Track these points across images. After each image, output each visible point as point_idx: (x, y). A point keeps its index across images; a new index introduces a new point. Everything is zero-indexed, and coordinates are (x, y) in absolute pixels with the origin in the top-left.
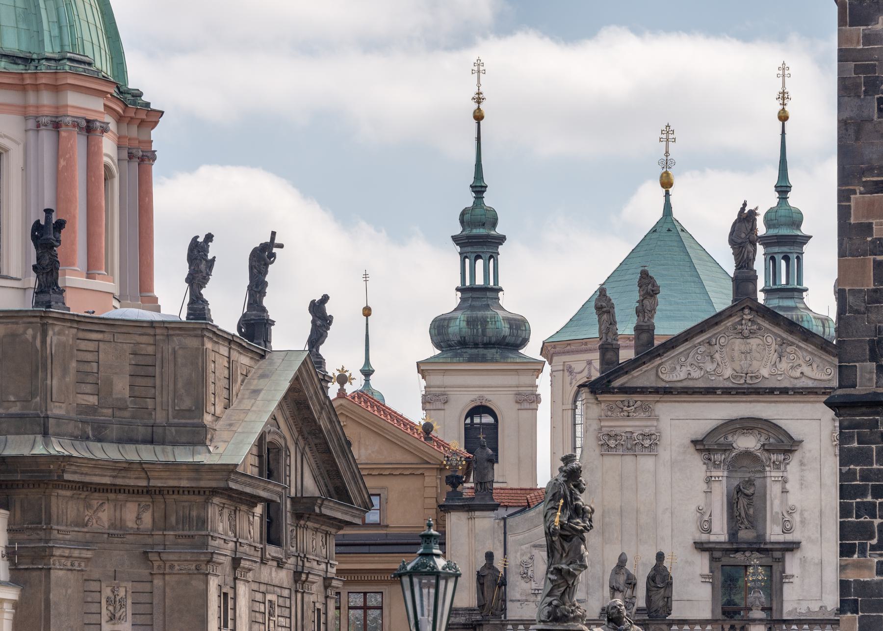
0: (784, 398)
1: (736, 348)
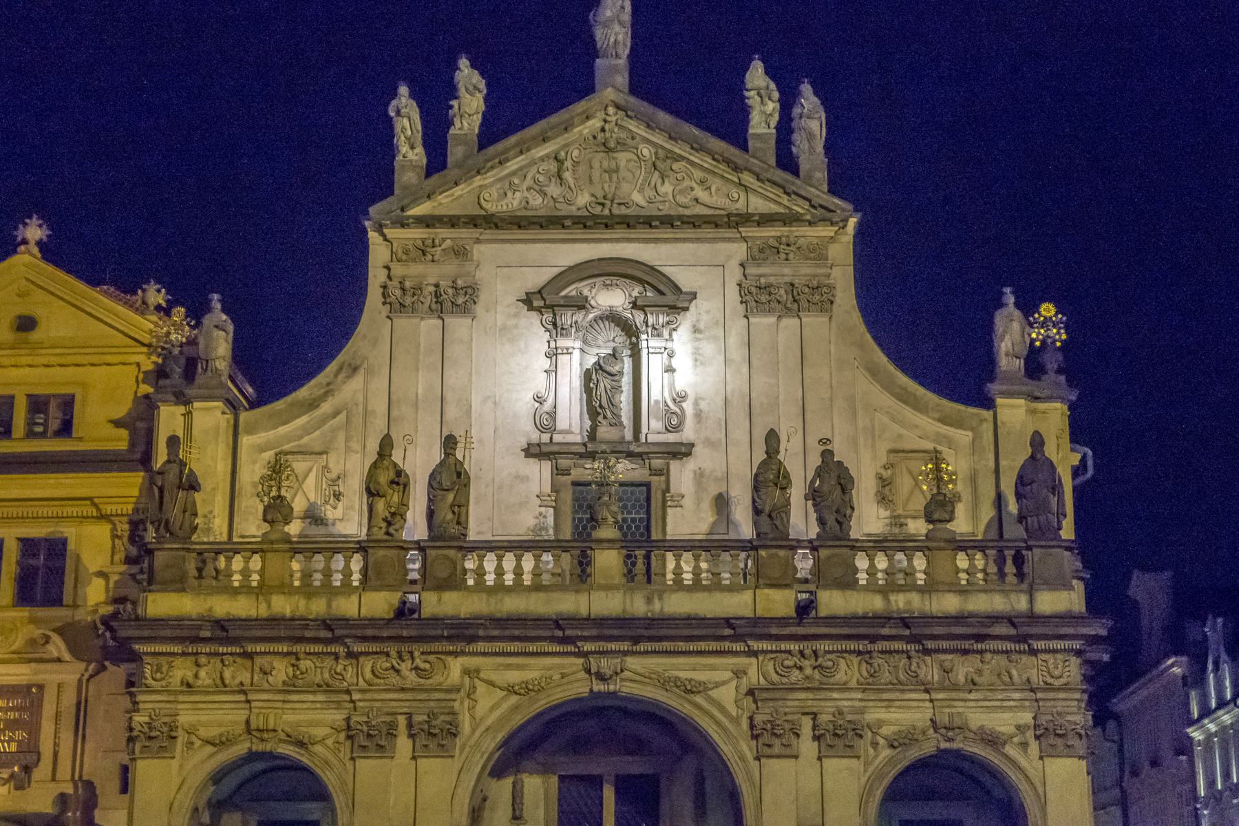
1: (596, 165)
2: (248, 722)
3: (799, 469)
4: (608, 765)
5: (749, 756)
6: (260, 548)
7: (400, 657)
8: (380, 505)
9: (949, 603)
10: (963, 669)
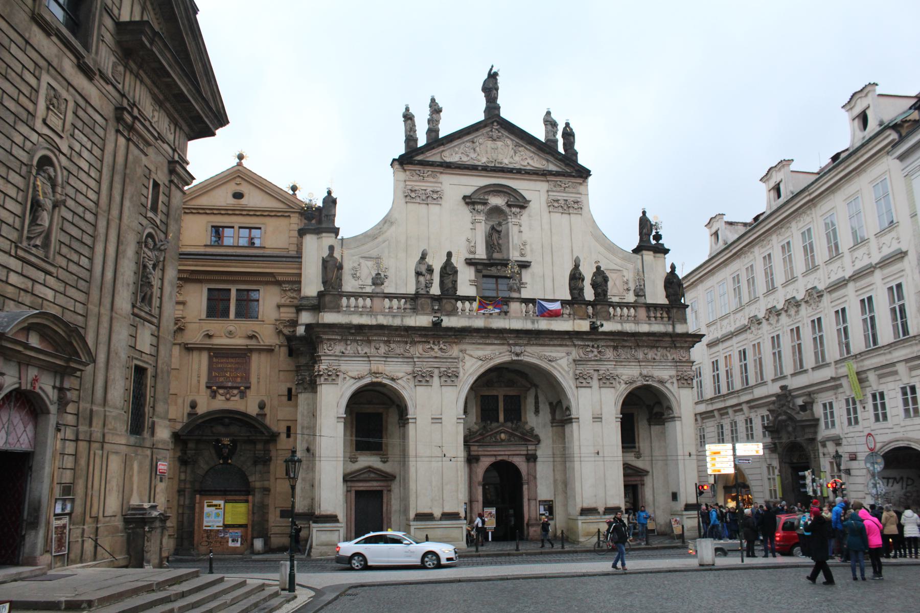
0: (518, 176)
2: (370, 370)
3: (588, 272)
4: (501, 392)
5: (573, 387)
6: (371, 296)
7: (434, 343)
8: (421, 279)
9: (644, 328)
10: (651, 354)
